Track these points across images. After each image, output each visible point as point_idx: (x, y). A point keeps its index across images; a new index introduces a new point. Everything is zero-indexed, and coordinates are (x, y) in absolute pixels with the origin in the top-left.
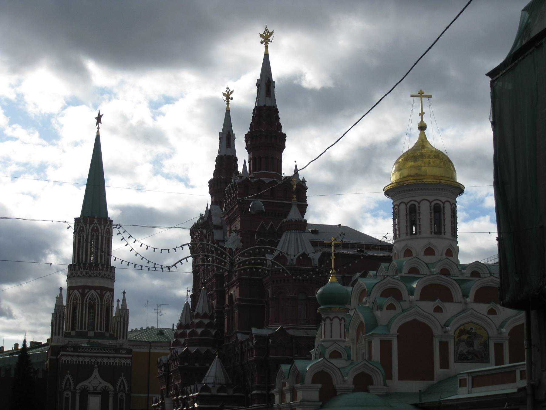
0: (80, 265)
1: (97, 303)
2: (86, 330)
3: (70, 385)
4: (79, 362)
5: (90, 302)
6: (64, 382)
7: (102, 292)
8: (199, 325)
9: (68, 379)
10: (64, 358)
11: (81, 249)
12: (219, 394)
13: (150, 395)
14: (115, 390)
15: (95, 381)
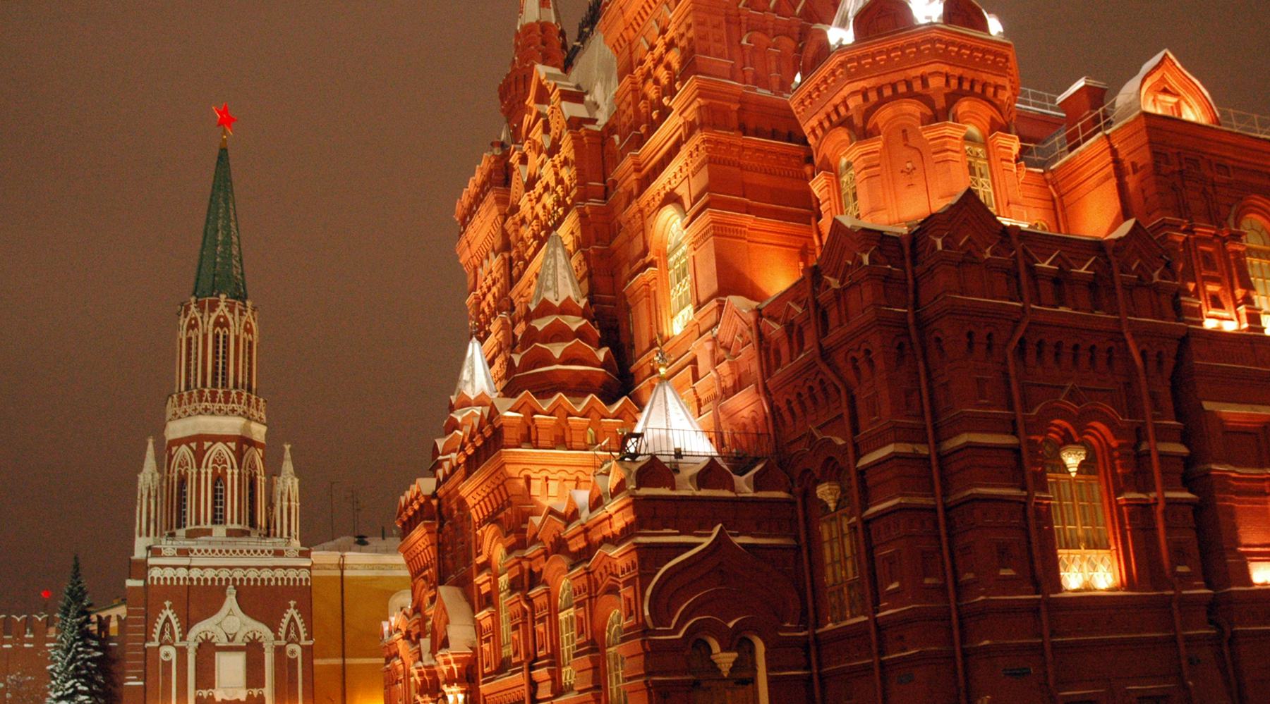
0: (190, 395)
1: (229, 465)
2: (209, 525)
3: (172, 633)
4: (191, 579)
5: (215, 469)
6: (159, 627)
7: (239, 447)
8: (557, 334)
9: (168, 620)
10: (155, 573)
11: (193, 368)
12: (704, 493)
13: (348, 661)
14: (277, 638)
15: (231, 621)
